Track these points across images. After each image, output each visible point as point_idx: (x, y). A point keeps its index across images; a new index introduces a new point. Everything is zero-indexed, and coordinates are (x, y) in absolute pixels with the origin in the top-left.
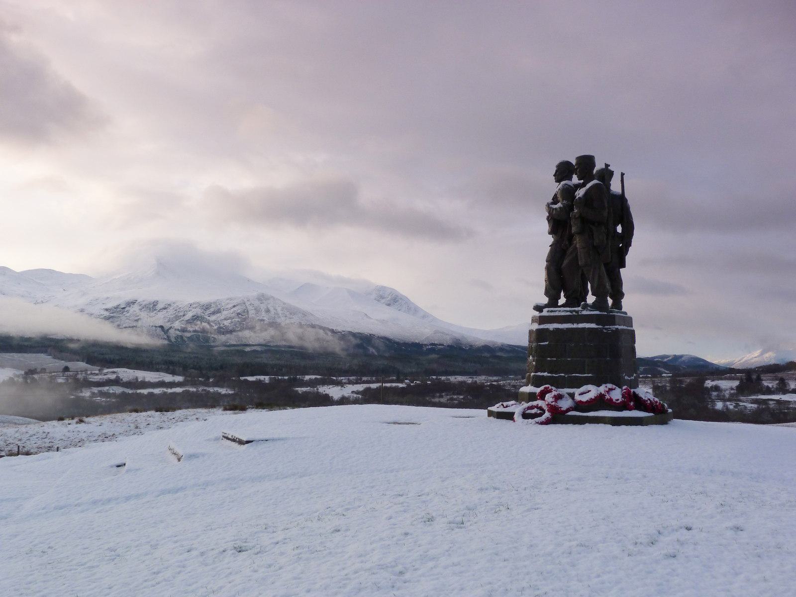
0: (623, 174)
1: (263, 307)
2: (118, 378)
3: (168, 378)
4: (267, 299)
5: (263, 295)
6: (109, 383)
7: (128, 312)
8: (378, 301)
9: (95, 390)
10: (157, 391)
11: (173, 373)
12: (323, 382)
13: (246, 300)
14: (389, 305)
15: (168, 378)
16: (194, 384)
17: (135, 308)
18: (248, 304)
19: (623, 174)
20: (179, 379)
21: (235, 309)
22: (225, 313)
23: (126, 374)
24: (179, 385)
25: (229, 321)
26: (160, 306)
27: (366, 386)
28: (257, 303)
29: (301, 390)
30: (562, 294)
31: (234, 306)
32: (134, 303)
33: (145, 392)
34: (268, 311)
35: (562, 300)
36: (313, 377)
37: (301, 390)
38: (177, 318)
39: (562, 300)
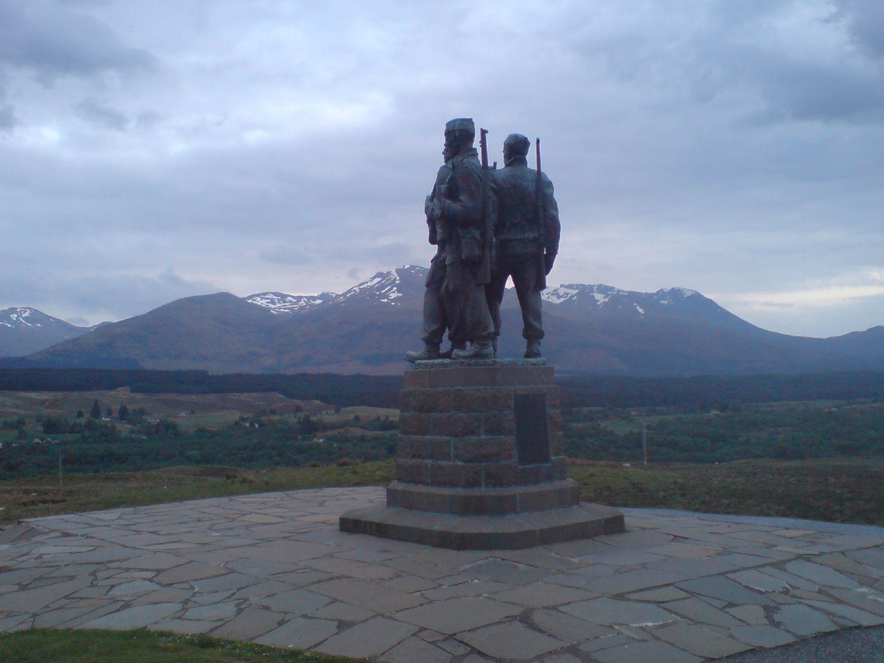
0: (538, 141)
2: (357, 418)
19: (538, 141)
23: (366, 412)
30: (447, 332)
33: (387, 433)
35: (446, 345)
39: (446, 345)
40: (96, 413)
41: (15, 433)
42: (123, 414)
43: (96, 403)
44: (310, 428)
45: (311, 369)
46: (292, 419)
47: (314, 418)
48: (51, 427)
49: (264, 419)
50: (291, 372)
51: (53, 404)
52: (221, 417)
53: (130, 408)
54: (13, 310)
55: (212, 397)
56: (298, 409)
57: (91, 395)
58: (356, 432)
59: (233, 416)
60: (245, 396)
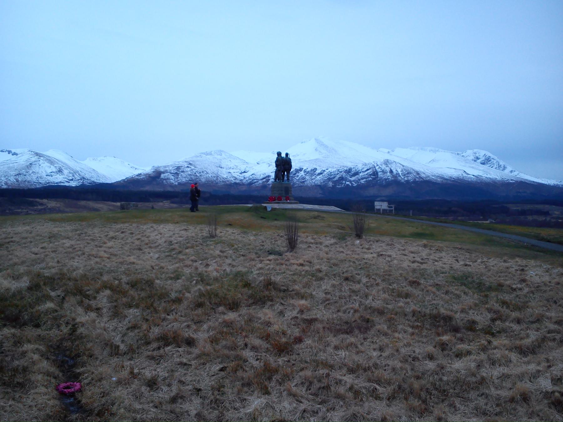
1: (388, 169)
4: (391, 163)
5: (388, 161)
7: (298, 176)
8: (475, 161)
13: (376, 165)
14: (483, 164)
17: (302, 173)
18: (377, 168)
21: (368, 171)
22: (361, 174)
25: (365, 180)
26: (318, 171)
28: (384, 167)
31: (368, 170)
32: (301, 170)
34: (391, 171)
38: (329, 179)
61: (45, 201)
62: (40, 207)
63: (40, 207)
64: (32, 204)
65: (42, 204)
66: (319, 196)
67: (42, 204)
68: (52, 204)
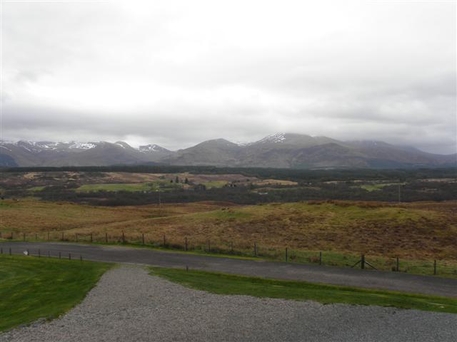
3: (291, 183)
6: (266, 186)
9: (261, 189)
10: (286, 189)
11: (293, 181)
12: (363, 184)
15: (291, 183)
16: (302, 185)
20: (296, 183)
23: (271, 181)
24: (296, 186)
27: (384, 185)
29: (352, 187)
33: (281, 189)
36: (358, 181)
37: (352, 187)
40: (177, 181)
41: (150, 187)
42: (187, 182)
43: (177, 178)
44: (252, 187)
45: (253, 166)
46: (246, 184)
47: (254, 184)
48: (162, 185)
49: (236, 184)
50: (245, 166)
51: (163, 178)
52: (220, 183)
53: (189, 179)
54: (150, 146)
55: (217, 176)
56: (248, 180)
57: (175, 175)
58: (269, 189)
59: (223, 183)
60: (228, 175)
61: (111, 173)
62: (107, 178)
63: (107, 178)
64: (103, 176)
65: (109, 176)
66: (288, 167)
67: (109, 176)
68: (114, 175)
